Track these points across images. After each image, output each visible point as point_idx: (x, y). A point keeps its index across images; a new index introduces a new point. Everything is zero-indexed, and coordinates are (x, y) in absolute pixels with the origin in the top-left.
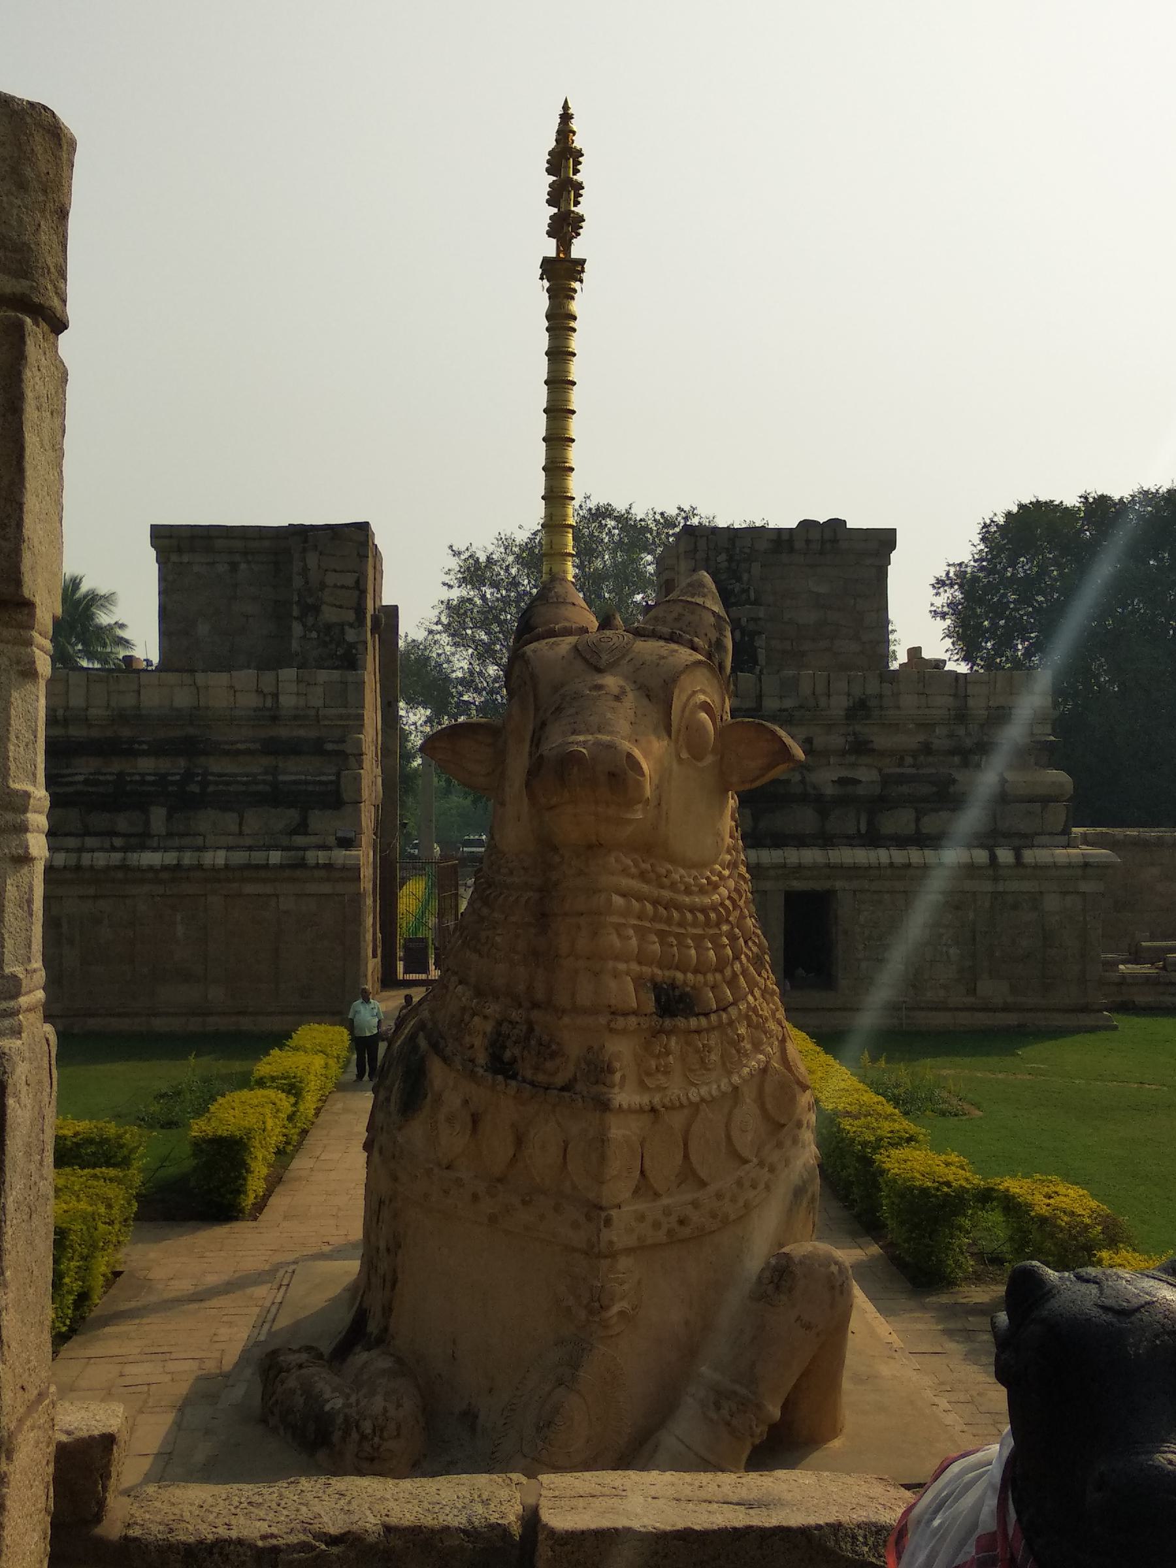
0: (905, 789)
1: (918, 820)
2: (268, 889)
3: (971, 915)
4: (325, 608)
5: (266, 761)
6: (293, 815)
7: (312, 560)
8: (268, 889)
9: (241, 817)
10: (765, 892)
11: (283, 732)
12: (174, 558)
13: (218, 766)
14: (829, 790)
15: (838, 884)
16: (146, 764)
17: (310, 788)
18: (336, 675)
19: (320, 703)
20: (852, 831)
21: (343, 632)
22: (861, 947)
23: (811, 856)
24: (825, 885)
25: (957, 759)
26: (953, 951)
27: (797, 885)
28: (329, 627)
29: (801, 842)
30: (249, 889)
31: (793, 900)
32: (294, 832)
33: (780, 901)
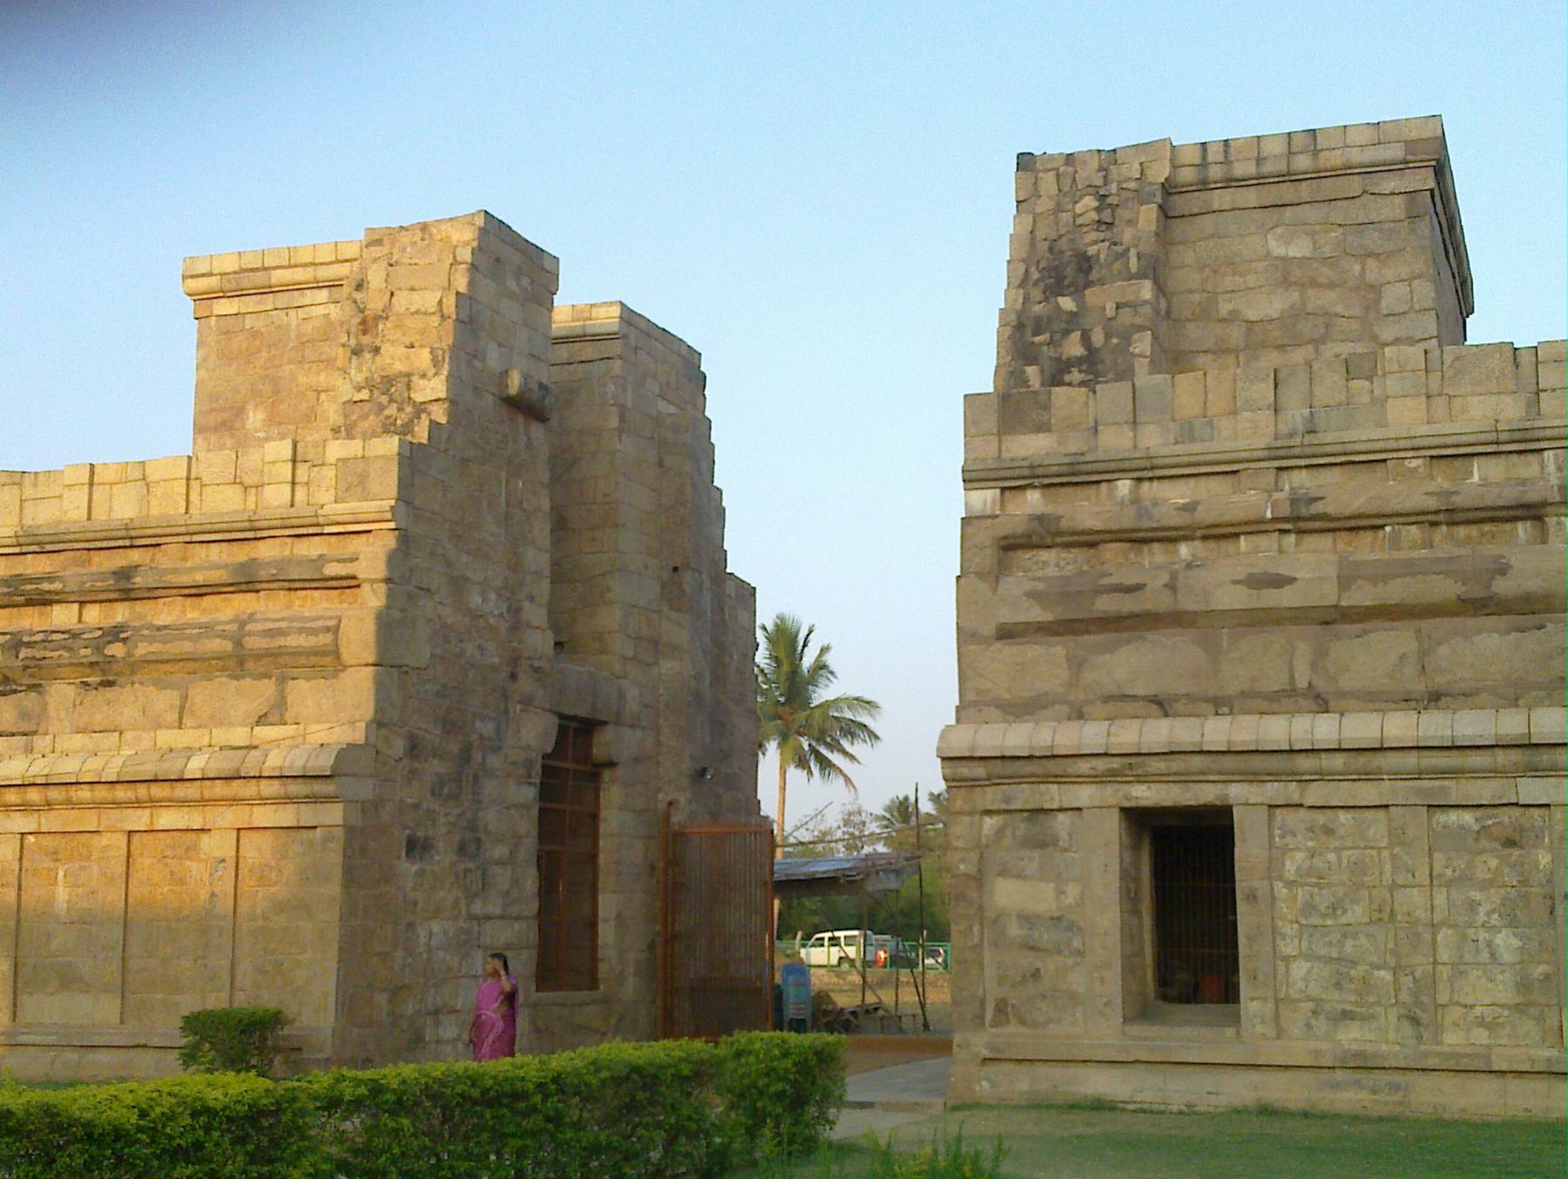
0: (1395, 592)
1: (1423, 654)
2: (195, 819)
3: (1544, 859)
4: (386, 349)
5: (242, 604)
6: (268, 687)
7: (376, 278)
8: (195, 819)
9: (185, 698)
10: (1079, 809)
11: (266, 551)
12: (223, 307)
13: (165, 613)
14: (1231, 598)
15: (1236, 793)
16: (62, 616)
17: (292, 641)
18: (354, 447)
19: (330, 496)
20: (1275, 680)
21: (409, 388)
22: (1289, 929)
23: (1159, 732)
24: (1205, 794)
25: (1523, 530)
26: (1507, 942)
27: (1146, 795)
28: (389, 381)
29: (1162, 705)
30: (167, 819)
31: (1144, 823)
32: (262, 720)
33: (1112, 825)
